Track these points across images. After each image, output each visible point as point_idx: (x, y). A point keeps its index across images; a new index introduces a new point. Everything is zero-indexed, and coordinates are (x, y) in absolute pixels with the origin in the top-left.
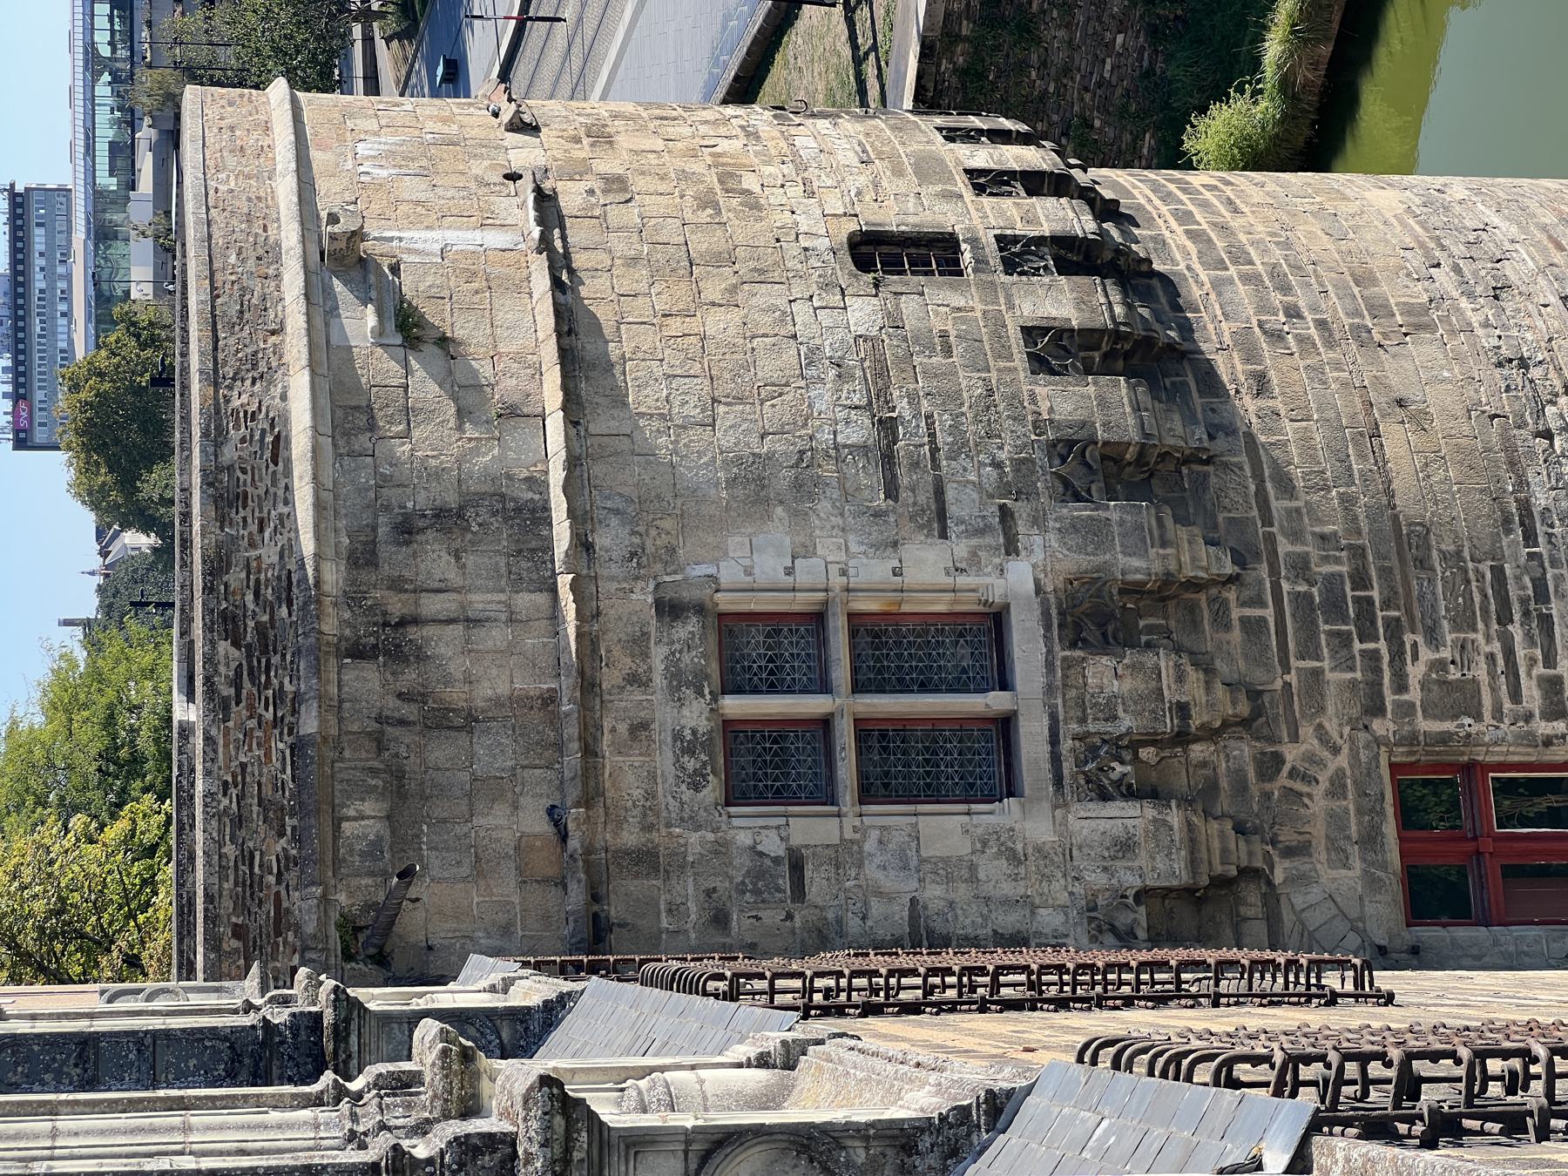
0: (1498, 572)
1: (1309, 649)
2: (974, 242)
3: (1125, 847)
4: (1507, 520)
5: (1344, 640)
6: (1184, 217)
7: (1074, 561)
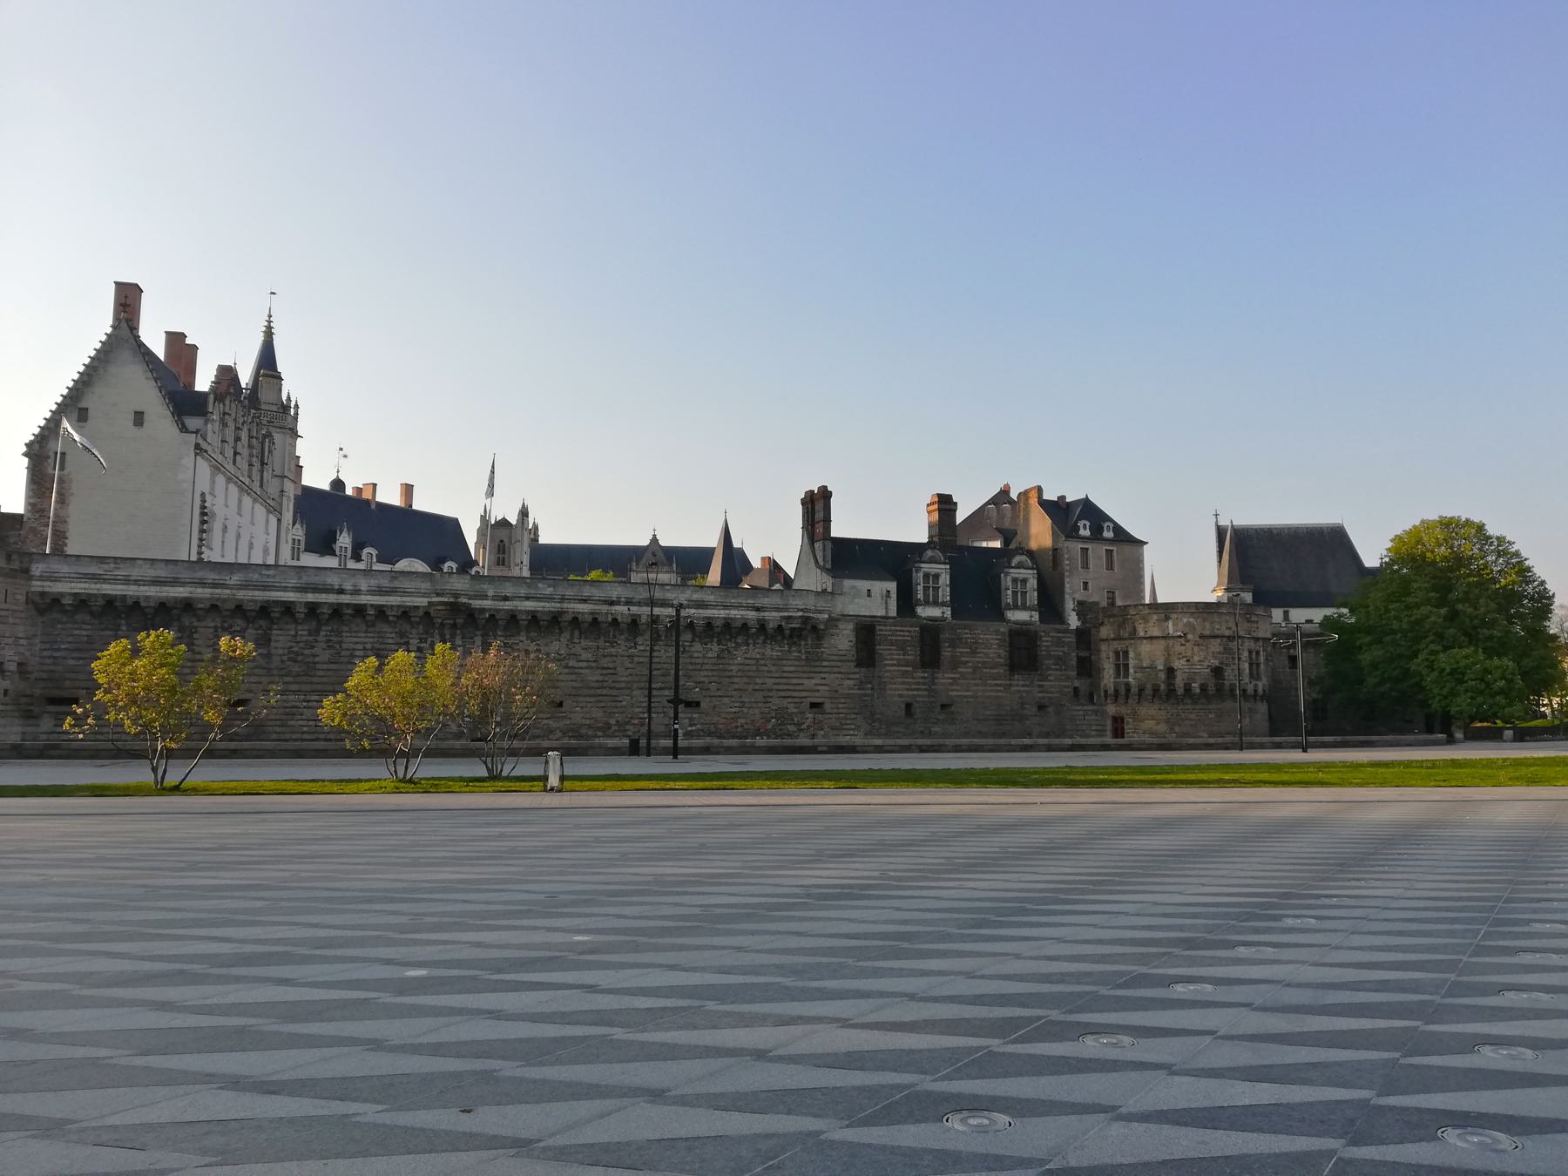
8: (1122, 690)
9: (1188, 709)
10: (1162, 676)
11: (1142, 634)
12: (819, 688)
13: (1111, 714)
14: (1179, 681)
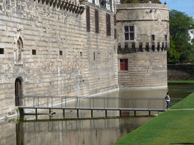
3: (123, 45)
7: (136, 43)
8: (130, 46)
9: (157, 54)
10: (150, 39)
11: (141, 19)
12: (82, 43)
14: (156, 42)
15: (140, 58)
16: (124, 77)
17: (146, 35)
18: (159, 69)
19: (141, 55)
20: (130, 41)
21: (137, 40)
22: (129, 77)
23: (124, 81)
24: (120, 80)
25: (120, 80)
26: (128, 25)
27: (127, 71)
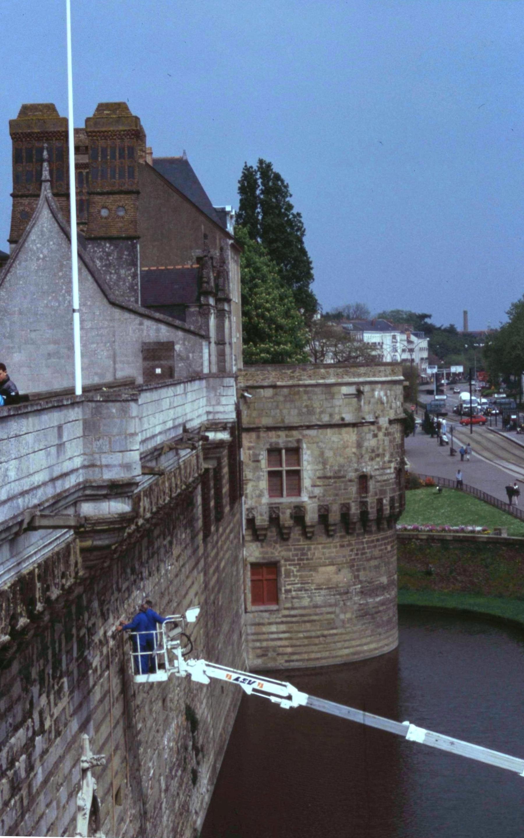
0: (308, 583)
1: (295, 549)
2: (366, 497)
4: (319, 586)
5: (297, 555)
6: (378, 540)
9: (373, 541)
10: (353, 489)
13: (252, 559)
15: (321, 558)
16: (264, 629)
17: (340, 477)
18: (378, 593)
19: (324, 548)
20: (286, 500)
21: (310, 498)
22: (283, 627)
23: (265, 644)
24: (254, 641)
25: (254, 641)
26: (282, 445)
27: (274, 607)
